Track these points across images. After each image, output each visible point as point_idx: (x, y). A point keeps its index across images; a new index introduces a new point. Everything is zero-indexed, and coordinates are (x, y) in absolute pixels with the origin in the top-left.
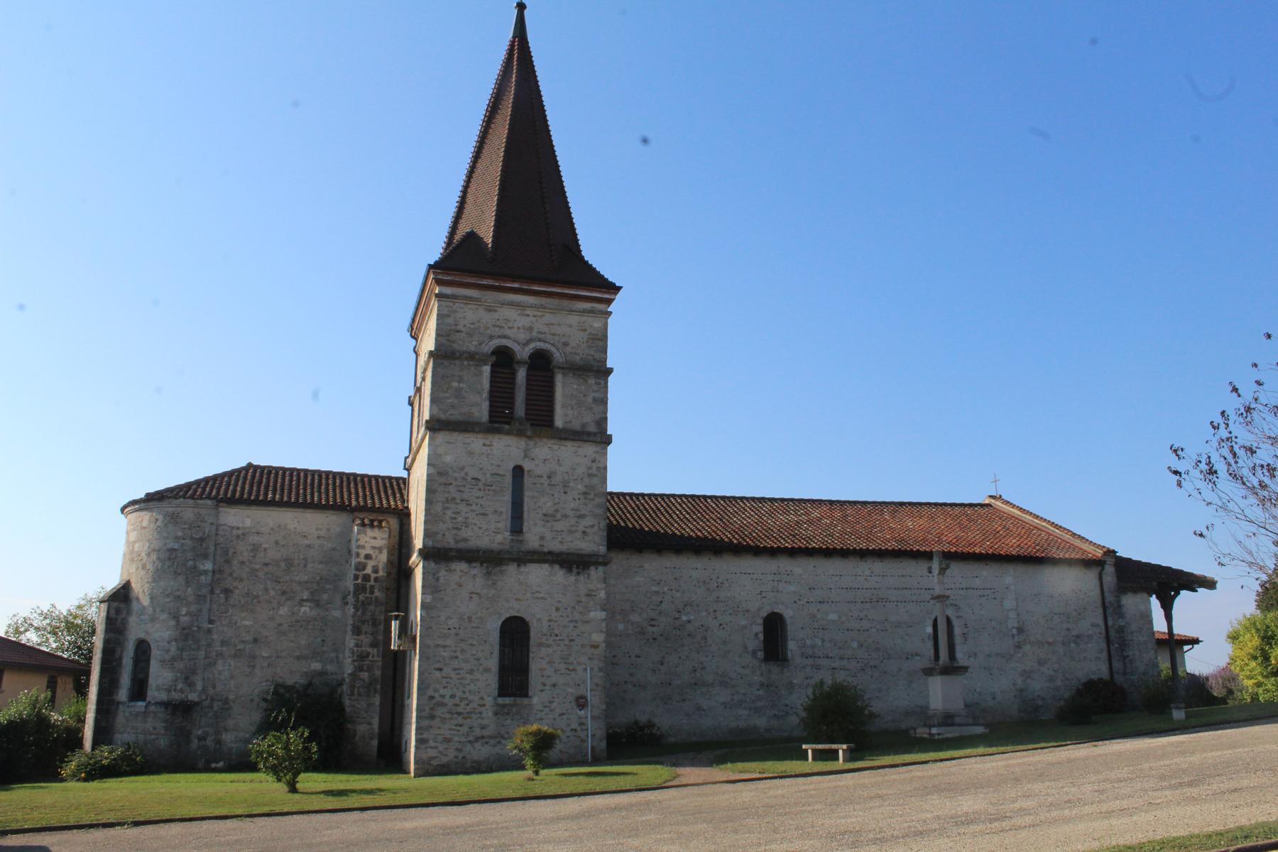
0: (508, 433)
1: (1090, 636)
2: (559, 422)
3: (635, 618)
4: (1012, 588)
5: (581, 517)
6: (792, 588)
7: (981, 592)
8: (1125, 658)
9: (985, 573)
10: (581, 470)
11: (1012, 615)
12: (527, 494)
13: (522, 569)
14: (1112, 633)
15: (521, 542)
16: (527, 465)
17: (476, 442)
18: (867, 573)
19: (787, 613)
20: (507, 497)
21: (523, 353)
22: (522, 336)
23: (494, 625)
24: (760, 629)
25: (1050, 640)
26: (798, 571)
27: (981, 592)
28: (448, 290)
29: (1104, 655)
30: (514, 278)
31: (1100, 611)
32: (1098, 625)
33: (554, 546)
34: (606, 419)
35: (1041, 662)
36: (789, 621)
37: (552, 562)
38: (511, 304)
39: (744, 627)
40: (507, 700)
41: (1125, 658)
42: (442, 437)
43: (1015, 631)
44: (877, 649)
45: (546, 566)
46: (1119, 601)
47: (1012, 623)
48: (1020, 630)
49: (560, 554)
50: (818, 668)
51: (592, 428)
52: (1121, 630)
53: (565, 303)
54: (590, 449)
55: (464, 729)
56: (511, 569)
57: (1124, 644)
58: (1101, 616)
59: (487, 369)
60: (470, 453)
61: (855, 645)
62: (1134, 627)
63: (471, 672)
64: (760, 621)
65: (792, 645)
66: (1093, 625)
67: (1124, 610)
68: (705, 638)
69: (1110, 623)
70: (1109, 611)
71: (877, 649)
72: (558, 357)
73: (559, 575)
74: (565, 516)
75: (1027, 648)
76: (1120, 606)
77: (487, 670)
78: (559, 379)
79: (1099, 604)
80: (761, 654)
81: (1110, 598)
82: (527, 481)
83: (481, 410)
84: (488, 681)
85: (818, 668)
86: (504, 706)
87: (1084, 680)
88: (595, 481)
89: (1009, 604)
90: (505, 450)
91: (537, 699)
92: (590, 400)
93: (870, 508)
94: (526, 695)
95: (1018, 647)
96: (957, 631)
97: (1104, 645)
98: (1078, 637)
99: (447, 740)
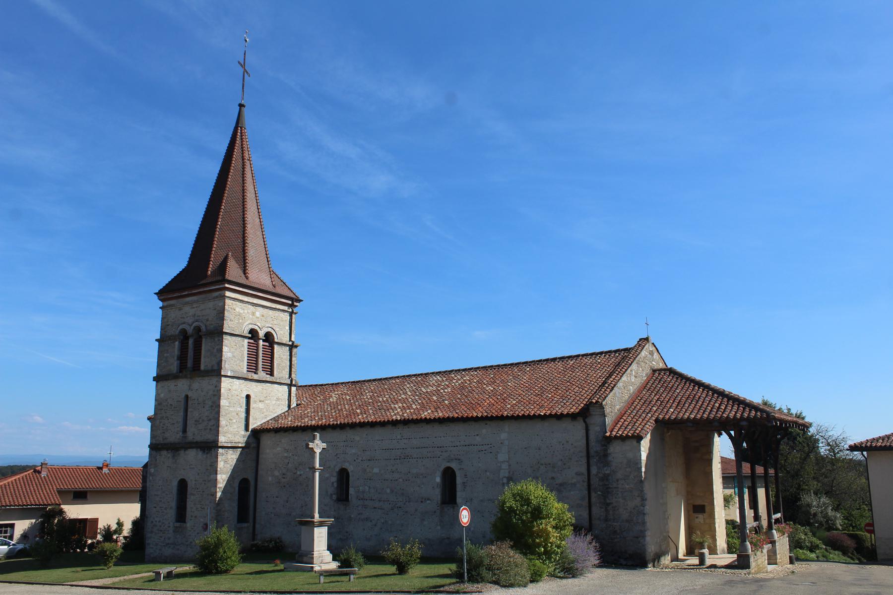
0: (182, 378)
1: (575, 484)
2: (202, 368)
3: (277, 473)
4: (506, 442)
5: (210, 420)
6: (354, 451)
8: (608, 504)
9: (484, 431)
10: (211, 393)
11: (505, 466)
12: (189, 410)
13: (187, 452)
14: (595, 481)
15: (185, 437)
16: (190, 394)
17: (171, 384)
18: (399, 437)
19: (350, 469)
20: (182, 414)
21: (190, 330)
22: (190, 321)
23: (175, 483)
24: (334, 479)
26: (357, 438)
28: (166, 304)
29: (585, 503)
30: (184, 289)
31: (584, 461)
32: (583, 474)
33: (198, 438)
34: (221, 360)
36: (350, 474)
37: (197, 448)
38: (187, 303)
39: (327, 478)
40: (178, 524)
41: (608, 504)
42: (161, 384)
43: (505, 481)
44: (403, 494)
45: (195, 450)
46: (606, 450)
49: (201, 442)
50: (365, 507)
51: (216, 368)
52: (605, 478)
53: (208, 295)
54: (214, 380)
55: (162, 539)
56: (182, 452)
57: (607, 491)
58: (586, 465)
59: (177, 343)
60: (170, 391)
61: (388, 491)
63: (166, 509)
64: (335, 474)
65: (352, 491)
66: (577, 474)
67: (610, 458)
68: (307, 486)
69: (594, 470)
70: (593, 461)
71: (403, 494)
72: (203, 328)
73: (200, 453)
74: (203, 421)
76: (606, 455)
77: (171, 508)
78: (204, 340)
79: (585, 454)
80: (334, 497)
81: (595, 447)
82: (190, 403)
83: (174, 366)
84: (172, 513)
85: (365, 507)
86: (177, 527)
88: (216, 398)
89: (502, 457)
90: (182, 386)
91: (189, 524)
92: (215, 351)
93: (476, 376)
94: (185, 522)
96: (459, 480)
98: (561, 485)
99: (157, 545)
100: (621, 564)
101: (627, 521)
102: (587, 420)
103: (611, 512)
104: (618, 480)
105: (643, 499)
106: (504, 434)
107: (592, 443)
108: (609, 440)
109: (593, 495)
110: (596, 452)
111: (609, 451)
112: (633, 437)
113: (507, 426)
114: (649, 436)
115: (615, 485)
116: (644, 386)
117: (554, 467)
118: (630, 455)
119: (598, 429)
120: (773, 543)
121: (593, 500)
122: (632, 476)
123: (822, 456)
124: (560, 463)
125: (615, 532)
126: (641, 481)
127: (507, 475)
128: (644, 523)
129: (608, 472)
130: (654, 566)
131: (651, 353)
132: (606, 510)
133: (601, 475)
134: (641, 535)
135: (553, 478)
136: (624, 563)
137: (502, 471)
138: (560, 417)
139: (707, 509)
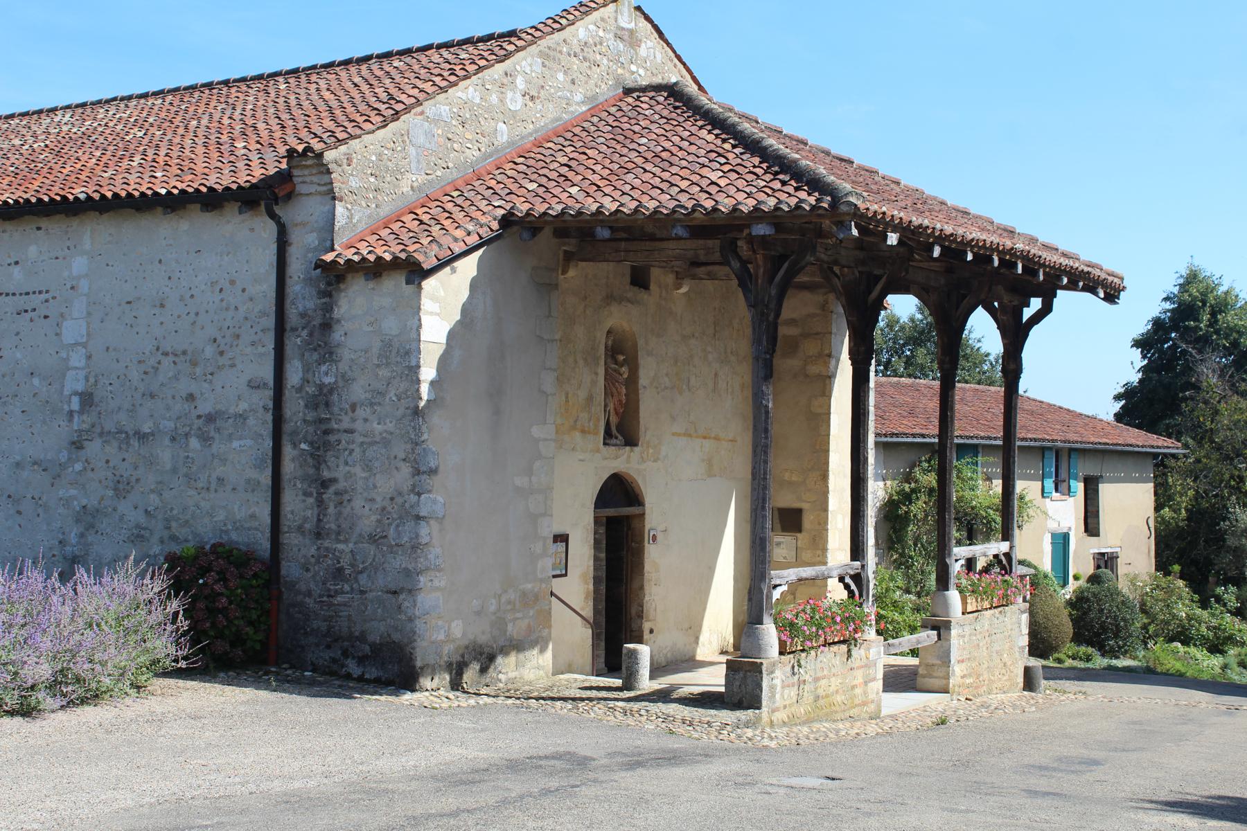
1: (242, 417)
4: (84, 285)
7: (21, 302)
8: (325, 484)
9: (33, 251)
11: (77, 359)
14: (294, 408)
25: (146, 428)
27: (21, 302)
29: (266, 478)
35: (121, 488)
41: (325, 484)
43: (75, 404)
46: (328, 309)
47: (75, 383)
48: (87, 400)
52: (322, 399)
57: (323, 443)
62: (358, 391)
67: (337, 335)
69: (294, 375)
70: (293, 343)
75: (93, 447)
76: (327, 326)
79: (270, 322)
81: (302, 297)
87: (210, 539)
89: (73, 330)
95: (77, 445)
97: (269, 443)
98: (210, 418)
100: (348, 677)
101: (373, 539)
102: (287, 213)
103: (331, 510)
104: (353, 408)
105: (422, 471)
106: (82, 254)
107: (295, 287)
108: (334, 276)
109: (288, 451)
110: (303, 315)
111: (337, 313)
112: (396, 264)
113: (93, 235)
114: (468, 267)
115: (346, 424)
116: (566, 134)
117: (194, 364)
118: (391, 325)
119: (312, 239)
120: (941, 628)
121: (288, 467)
122: (392, 394)
123: (1141, 381)
124: (209, 351)
125: (338, 573)
126: (416, 412)
127: (80, 387)
128: (416, 547)
129: (328, 380)
130: (456, 685)
131: (631, 39)
132: (320, 503)
133: (311, 390)
134: (403, 589)
135: (191, 397)
136: (356, 670)
137: (70, 374)
138: (211, 200)
139: (808, 521)
